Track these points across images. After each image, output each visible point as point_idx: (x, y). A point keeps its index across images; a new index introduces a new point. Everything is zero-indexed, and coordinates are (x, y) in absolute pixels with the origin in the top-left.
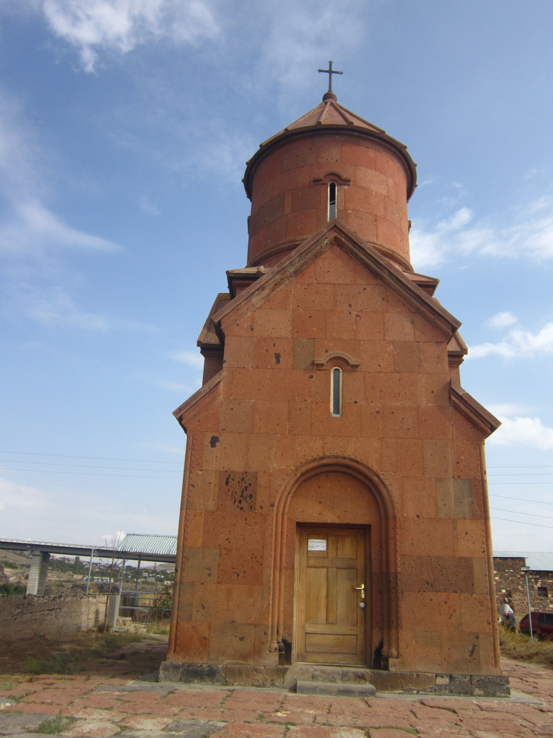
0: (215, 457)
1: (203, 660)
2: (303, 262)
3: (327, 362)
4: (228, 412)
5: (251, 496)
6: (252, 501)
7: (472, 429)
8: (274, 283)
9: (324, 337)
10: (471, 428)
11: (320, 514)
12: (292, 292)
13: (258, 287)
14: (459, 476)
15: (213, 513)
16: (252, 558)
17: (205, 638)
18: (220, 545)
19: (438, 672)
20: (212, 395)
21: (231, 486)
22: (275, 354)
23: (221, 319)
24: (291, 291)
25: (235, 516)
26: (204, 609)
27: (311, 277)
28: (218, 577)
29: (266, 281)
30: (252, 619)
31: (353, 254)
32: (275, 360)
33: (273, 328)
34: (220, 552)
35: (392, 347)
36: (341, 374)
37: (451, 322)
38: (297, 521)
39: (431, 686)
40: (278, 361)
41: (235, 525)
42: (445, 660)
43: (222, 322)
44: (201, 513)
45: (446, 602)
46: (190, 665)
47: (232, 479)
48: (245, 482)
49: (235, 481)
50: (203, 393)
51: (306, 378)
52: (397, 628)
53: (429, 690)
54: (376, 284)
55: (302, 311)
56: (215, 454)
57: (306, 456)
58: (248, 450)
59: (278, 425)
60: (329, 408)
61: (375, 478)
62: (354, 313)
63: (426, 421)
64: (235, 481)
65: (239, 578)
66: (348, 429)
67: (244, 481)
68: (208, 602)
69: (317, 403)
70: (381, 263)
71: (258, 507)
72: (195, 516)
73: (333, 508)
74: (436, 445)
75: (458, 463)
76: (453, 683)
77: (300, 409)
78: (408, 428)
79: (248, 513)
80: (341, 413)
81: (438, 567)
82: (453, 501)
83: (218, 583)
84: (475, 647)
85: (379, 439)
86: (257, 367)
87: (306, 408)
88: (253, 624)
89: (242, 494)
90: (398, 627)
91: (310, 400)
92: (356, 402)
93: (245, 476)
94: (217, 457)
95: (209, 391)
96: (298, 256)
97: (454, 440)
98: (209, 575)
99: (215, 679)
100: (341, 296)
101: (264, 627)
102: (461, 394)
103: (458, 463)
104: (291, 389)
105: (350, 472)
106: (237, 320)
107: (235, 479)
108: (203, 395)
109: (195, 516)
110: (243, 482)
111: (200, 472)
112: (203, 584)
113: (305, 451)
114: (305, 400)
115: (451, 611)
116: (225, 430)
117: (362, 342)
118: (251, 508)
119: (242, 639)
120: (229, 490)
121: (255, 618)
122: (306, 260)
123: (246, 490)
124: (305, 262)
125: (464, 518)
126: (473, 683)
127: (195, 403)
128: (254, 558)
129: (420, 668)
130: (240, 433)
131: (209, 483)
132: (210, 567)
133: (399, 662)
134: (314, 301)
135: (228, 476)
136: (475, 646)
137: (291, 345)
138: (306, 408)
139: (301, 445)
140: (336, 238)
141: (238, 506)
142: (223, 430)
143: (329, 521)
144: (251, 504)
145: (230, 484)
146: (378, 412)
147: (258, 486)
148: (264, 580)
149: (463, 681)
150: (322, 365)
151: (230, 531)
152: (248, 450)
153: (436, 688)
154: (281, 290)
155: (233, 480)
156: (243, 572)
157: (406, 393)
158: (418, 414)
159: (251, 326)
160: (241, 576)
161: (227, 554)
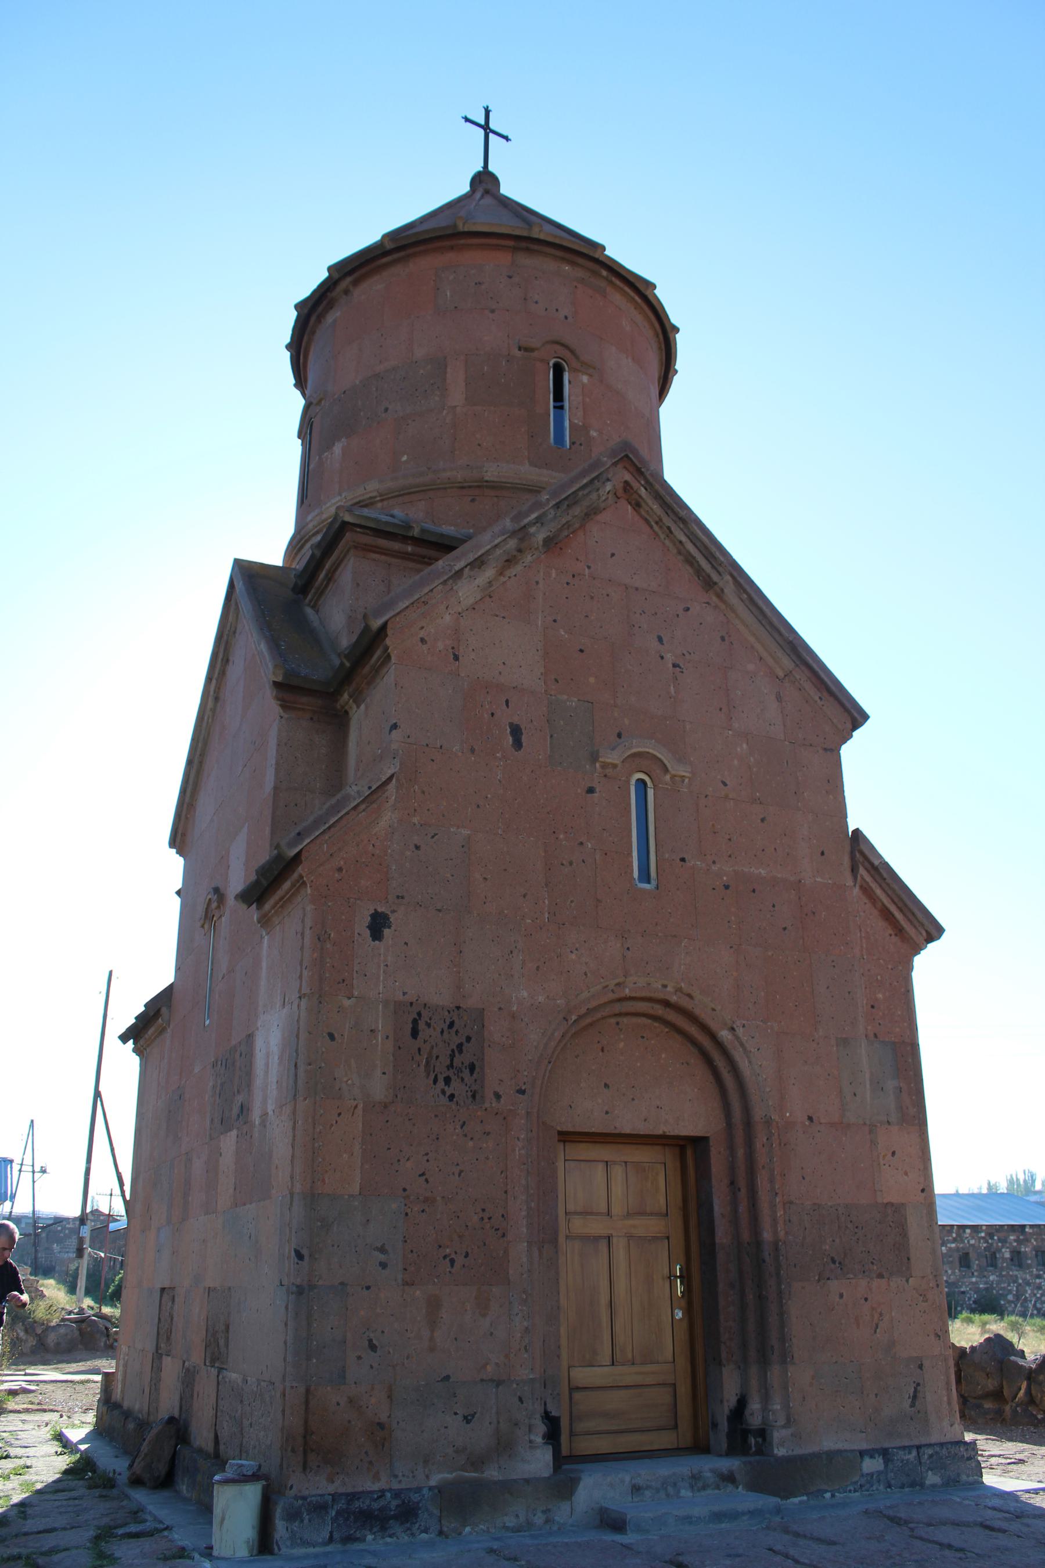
0: (382, 965)
1: (379, 1480)
2: (564, 521)
3: (623, 762)
4: (408, 853)
5: (472, 1068)
6: (476, 1080)
7: (893, 937)
8: (505, 558)
10: (891, 935)
11: (607, 1113)
12: (541, 585)
13: (471, 557)
14: (876, 1036)
15: (386, 1107)
16: (482, 1219)
17: (381, 1426)
18: (405, 1190)
19: (864, 1446)
21: (425, 1042)
22: (511, 725)
23: (390, 618)
24: (537, 583)
25: (436, 1116)
26: (376, 1352)
27: (577, 559)
28: (405, 1269)
29: (489, 547)
30: (489, 1368)
31: (661, 527)
32: (511, 738)
33: (504, 663)
34: (406, 1205)
35: (745, 746)
36: (650, 793)
37: (852, 711)
38: (559, 1129)
40: (518, 744)
41: (438, 1139)
43: (389, 625)
44: (356, 1107)
45: (866, 1299)
46: (352, 1497)
47: (427, 1022)
48: (457, 1032)
49: (434, 1029)
50: (355, 799)
51: (579, 791)
52: (784, 1362)
54: (708, 603)
55: (563, 633)
56: (382, 958)
57: (589, 975)
58: (461, 952)
59: (524, 896)
61: (724, 1035)
62: (669, 657)
63: (814, 913)
64: (434, 1029)
65: (453, 1271)
67: (454, 1029)
68: (383, 1332)
70: (722, 559)
72: (339, 1114)
73: (633, 1099)
74: (834, 966)
77: (571, 863)
79: (468, 1109)
81: (850, 1225)
82: (868, 1086)
83: (406, 1283)
84: (919, 1388)
85: (731, 947)
87: (583, 861)
88: (492, 1380)
89: (452, 1060)
90: (785, 1358)
94: (387, 965)
95: (368, 795)
96: (552, 507)
98: (383, 1265)
99: (417, 1526)
100: (641, 614)
101: (517, 1384)
102: (876, 863)
105: (672, 1016)
106: (422, 628)
107: (432, 1022)
108: (355, 803)
111: (347, 1003)
112: (368, 1288)
113: (586, 963)
114: (581, 843)
115: (876, 1316)
116: (402, 897)
117: (688, 727)
118: (474, 1096)
119: (467, 1419)
120: (419, 1050)
121: (497, 1364)
122: (569, 518)
123: (461, 1051)
124: (567, 522)
126: (923, 1461)
128: (486, 1220)
129: (829, 1443)
130: (440, 911)
131: (372, 1031)
134: (587, 616)
135: (416, 1016)
136: (918, 1384)
138: (583, 861)
139: (577, 950)
140: (626, 483)
141: (443, 1092)
142: (398, 897)
143: (627, 1130)
144: (474, 1088)
146: (727, 887)
148: (511, 1272)
150: (615, 766)
151: (427, 1154)
152: (461, 952)
154: (515, 575)
155: (428, 1025)
156: (464, 1254)
157: (775, 849)
158: (799, 898)
159: (453, 648)
160: (458, 1265)
161: (423, 1211)
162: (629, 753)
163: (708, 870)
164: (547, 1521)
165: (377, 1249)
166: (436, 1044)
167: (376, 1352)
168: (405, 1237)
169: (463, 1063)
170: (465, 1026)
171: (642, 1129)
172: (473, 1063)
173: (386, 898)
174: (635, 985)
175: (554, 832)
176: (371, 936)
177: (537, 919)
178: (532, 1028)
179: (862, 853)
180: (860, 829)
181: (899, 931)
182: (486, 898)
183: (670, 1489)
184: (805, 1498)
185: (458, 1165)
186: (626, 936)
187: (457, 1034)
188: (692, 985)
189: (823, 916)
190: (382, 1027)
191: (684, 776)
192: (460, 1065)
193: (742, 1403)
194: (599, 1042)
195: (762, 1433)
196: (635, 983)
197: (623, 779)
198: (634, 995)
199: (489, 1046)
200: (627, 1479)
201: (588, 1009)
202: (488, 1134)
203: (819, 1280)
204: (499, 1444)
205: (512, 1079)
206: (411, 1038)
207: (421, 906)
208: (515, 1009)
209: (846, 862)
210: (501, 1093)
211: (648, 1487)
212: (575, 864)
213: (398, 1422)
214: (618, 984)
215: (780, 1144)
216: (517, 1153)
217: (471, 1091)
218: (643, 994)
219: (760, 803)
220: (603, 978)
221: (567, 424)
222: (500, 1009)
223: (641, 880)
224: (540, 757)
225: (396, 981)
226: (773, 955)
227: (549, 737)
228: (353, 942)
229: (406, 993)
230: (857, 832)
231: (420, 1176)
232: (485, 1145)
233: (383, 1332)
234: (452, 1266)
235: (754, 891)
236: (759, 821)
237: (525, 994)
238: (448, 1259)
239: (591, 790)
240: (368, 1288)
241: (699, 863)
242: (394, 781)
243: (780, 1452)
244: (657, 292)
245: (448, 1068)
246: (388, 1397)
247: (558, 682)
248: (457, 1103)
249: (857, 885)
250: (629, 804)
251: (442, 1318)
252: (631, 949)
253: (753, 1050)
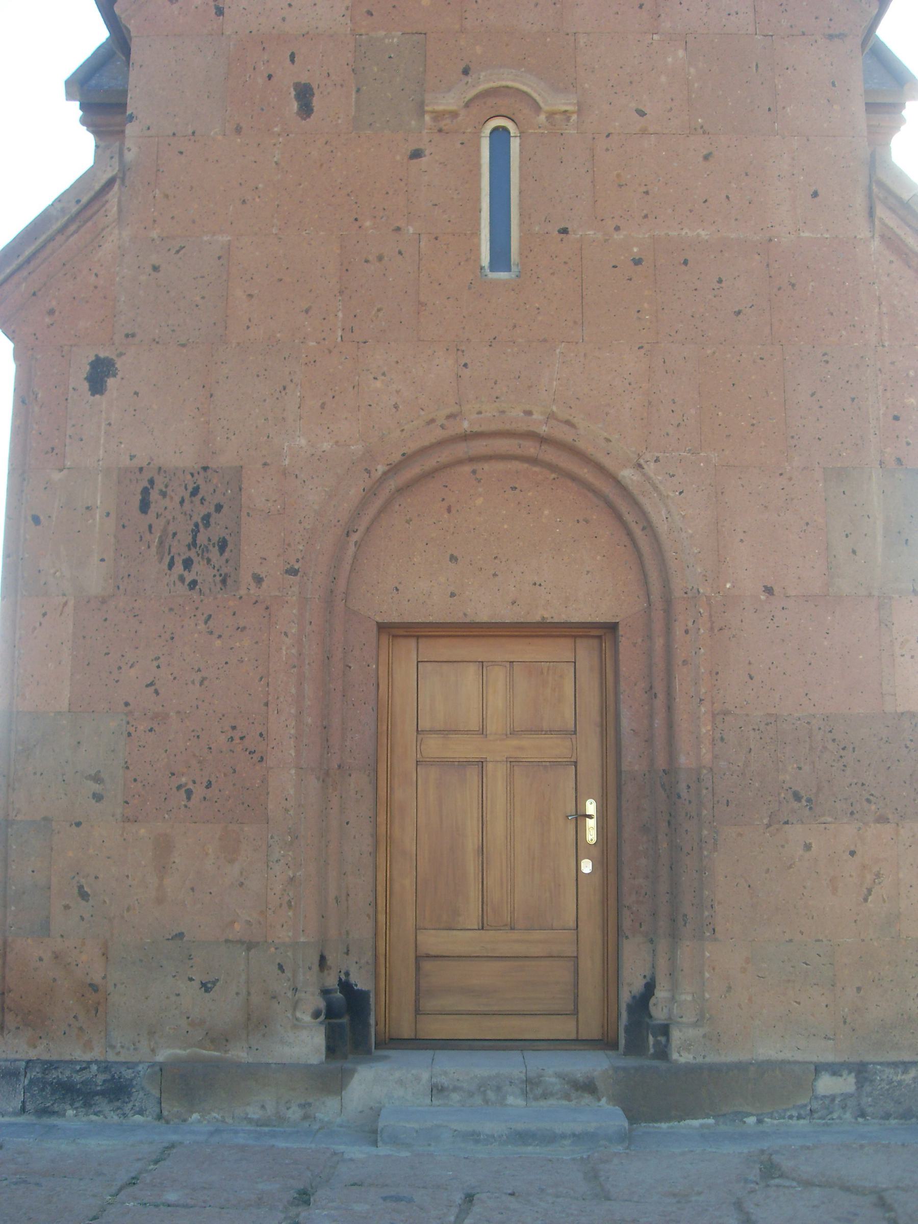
0: (103, 424)
1: (92, 1049)
3: (467, 105)
4: (143, 278)
5: (223, 545)
6: (227, 561)
9: (457, 27)
11: (453, 595)
14: (899, 461)
16: (232, 739)
17: (94, 988)
18: (127, 704)
20: (90, 224)
21: (158, 516)
22: (297, 86)
25: (171, 609)
26: (87, 901)
30: (237, 926)
32: (295, 106)
34: (128, 723)
35: (681, 53)
36: (515, 144)
39: (800, 1102)
40: (306, 109)
41: (172, 638)
42: (845, 1022)
44: (66, 604)
45: (853, 853)
46: (49, 1066)
47: (161, 491)
48: (203, 500)
51: (398, 158)
53: (795, 1113)
56: (104, 415)
58: (211, 396)
59: (307, 311)
60: (475, 250)
61: (627, 475)
64: (172, 498)
65: (190, 804)
66: (540, 318)
67: (199, 496)
69: (436, 239)
71: (246, 577)
72: (44, 615)
73: (495, 575)
74: (827, 362)
75: (896, 418)
76: (867, 1088)
77: (380, 258)
78: (737, 310)
79: (215, 598)
80: (513, 268)
82: (880, 539)
83: (127, 820)
86: (238, 130)
87: (400, 253)
88: (241, 942)
91: (411, 230)
92: (564, 231)
93: (201, 482)
94: (110, 424)
97: (883, 346)
98: (98, 797)
99: (130, 1105)
101: (276, 949)
103: (896, 418)
104: (348, 195)
105: (550, 455)
107: (169, 492)
109: (44, 615)
110: (197, 500)
111: (56, 476)
112: (78, 824)
113: (398, 392)
114: (398, 229)
115: (869, 877)
116: (133, 335)
117: (582, 40)
118: (224, 582)
119: (206, 987)
120: (150, 527)
121: (249, 923)
123: (207, 525)
127: (34, 255)
130: (184, 346)
131: (87, 508)
132: (99, 772)
133: (704, 1036)
135: (146, 484)
137: (350, 55)
138: (400, 253)
139: (384, 374)
141: (182, 579)
142: (127, 336)
143: (484, 616)
144: (224, 570)
145: (153, 509)
146: (637, 262)
147: (244, 514)
148: (270, 807)
149: (900, 1083)
150: (454, 115)
152: (211, 396)
153: (815, 1105)
155: (164, 494)
156: (205, 784)
157: (727, 197)
161: (151, 730)
162: (473, 93)
163: (606, 241)
164: (305, 1117)
165: (90, 777)
166: (174, 518)
167: (87, 901)
168: (126, 762)
169: (209, 540)
170: (215, 491)
171: (508, 615)
172: (224, 538)
173: (112, 339)
174: (480, 416)
175: (356, 220)
176: (90, 390)
177: (324, 339)
178: (310, 487)
179: (881, 185)
182: (250, 320)
183: (491, 1095)
185: (199, 670)
186: (463, 348)
187: (202, 503)
188: (570, 407)
189: (810, 288)
190: (101, 502)
191: (566, 112)
192: (206, 543)
194: (443, 500)
196: (480, 413)
197: (469, 130)
198: (476, 429)
199: (248, 514)
200: (425, 1076)
201: (403, 455)
202: (244, 628)
203: (769, 826)
204: (249, 1019)
205: (279, 556)
206: (139, 512)
207: (158, 343)
208: (287, 462)
209: (860, 201)
210: (263, 575)
211: (455, 1089)
212: (386, 258)
213: (115, 985)
214: (451, 416)
215: (712, 629)
216: (284, 653)
217: (221, 575)
218: (494, 427)
219: (704, 133)
220: (422, 409)
222: (265, 464)
223: (493, 267)
224: (340, 121)
225: (121, 443)
226: (714, 353)
227: (354, 93)
228: (67, 399)
229: (135, 456)
231: (147, 686)
232: (238, 644)
233: (96, 878)
234: (189, 798)
235: (686, 262)
236: (701, 159)
237: (303, 442)
238: (184, 789)
239: (416, 154)
240: (78, 824)
241: (591, 232)
242: (116, 187)
245: (189, 546)
246: (103, 955)
247: (372, 15)
248: (201, 591)
249: (876, 235)
250: (478, 165)
251: (174, 862)
252: (469, 365)
253: (671, 494)
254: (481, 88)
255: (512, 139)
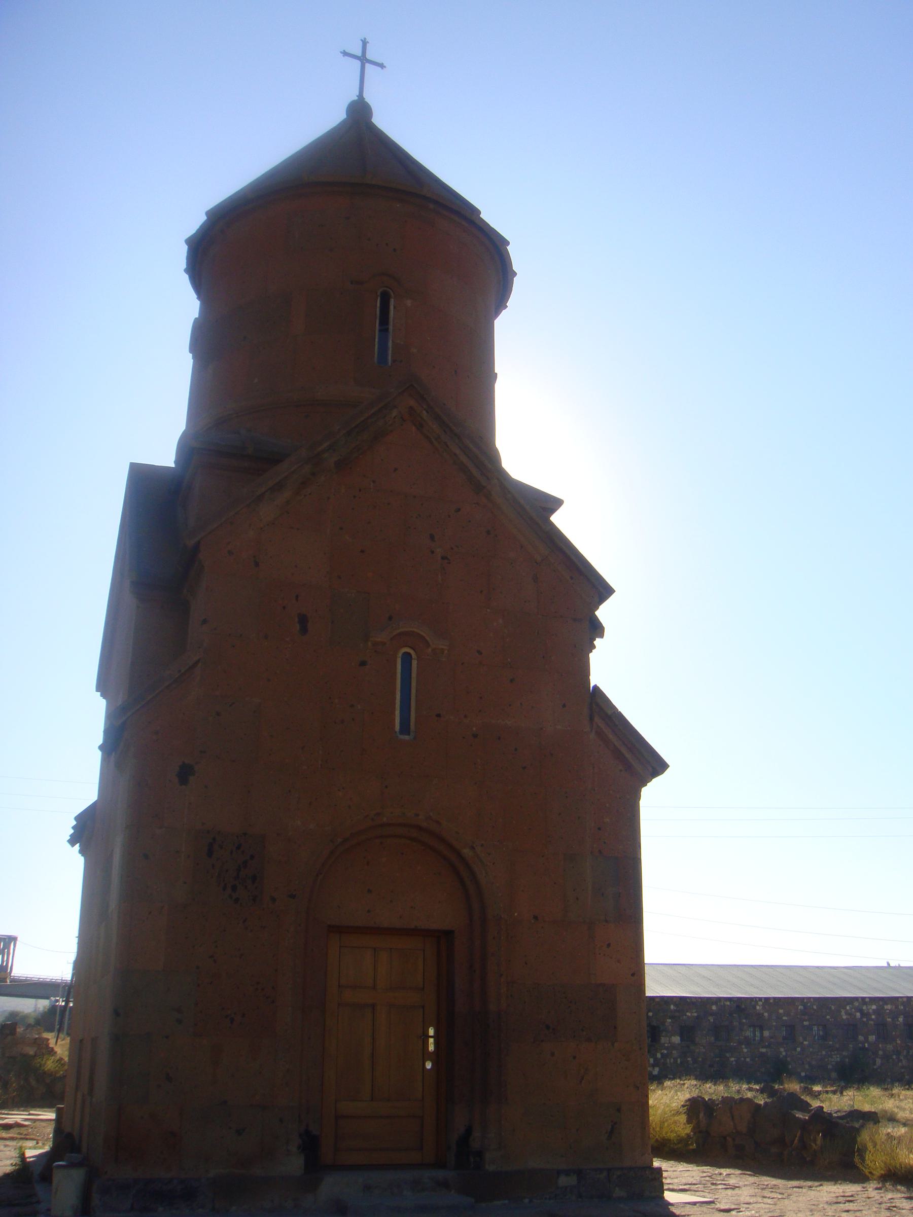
5: (254, 878)
14: (600, 852)
18: (198, 968)
32: (298, 626)
35: (501, 621)
36: (415, 663)
40: (304, 630)
45: (574, 1058)
61: (466, 852)
91: (359, 707)
92: (438, 716)
102: (609, 712)
103: (599, 829)
112: (167, 1037)
114: (352, 706)
120: (213, 866)
125: (606, 921)
136: (615, 1123)
139: (343, 788)
140: (411, 408)
146: (475, 736)
180: (598, 685)
181: (629, 767)
184: (506, 1202)
191: (443, 649)
193: (469, 1131)
195: (480, 1154)
196: (392, 813)
221: (390, 344)
230: (595, 687)
239: (363, 664)
243: (491, 1168)
244: (483, 216)
250: (395, 673)
254: (398, 631)
255: (413, 661)
